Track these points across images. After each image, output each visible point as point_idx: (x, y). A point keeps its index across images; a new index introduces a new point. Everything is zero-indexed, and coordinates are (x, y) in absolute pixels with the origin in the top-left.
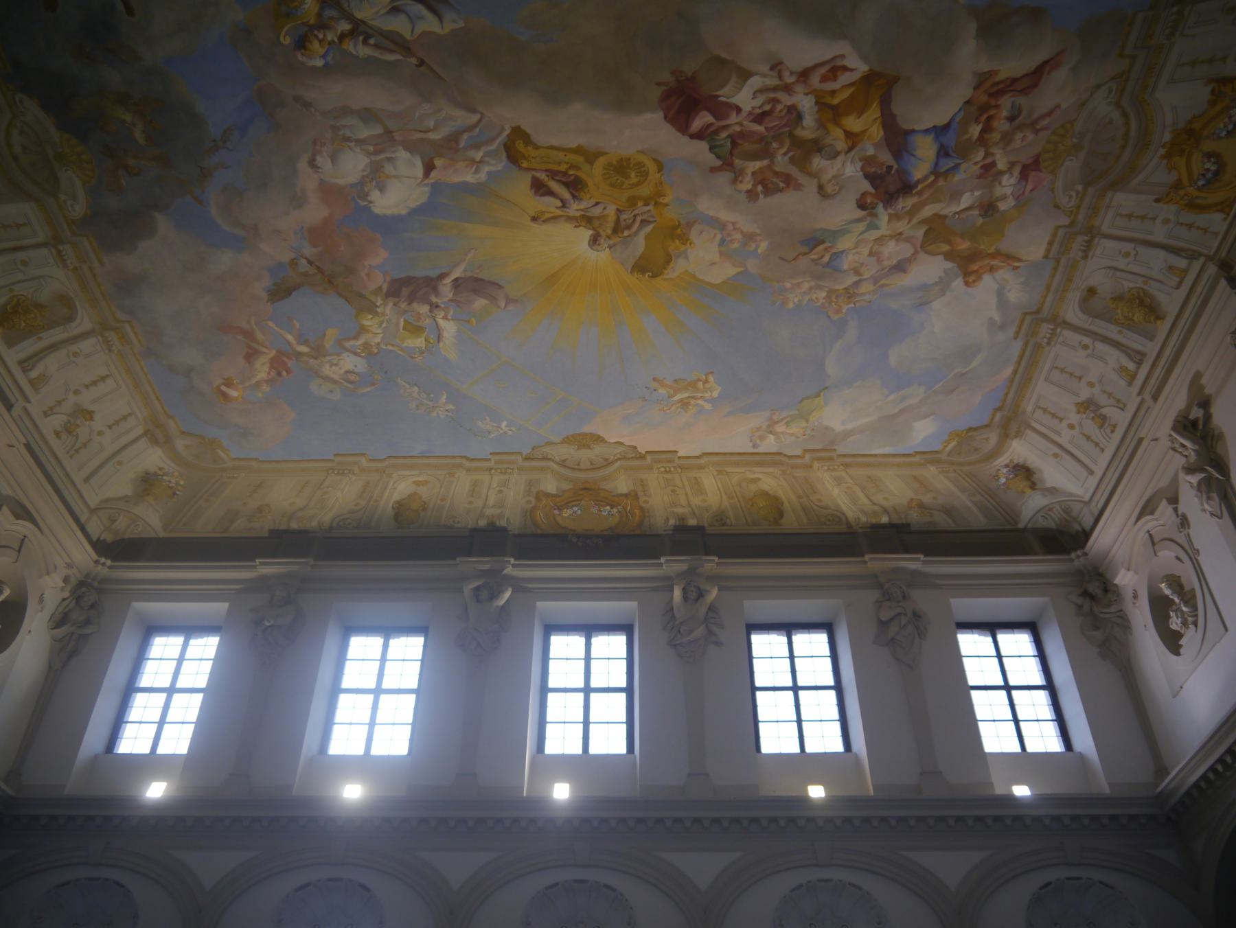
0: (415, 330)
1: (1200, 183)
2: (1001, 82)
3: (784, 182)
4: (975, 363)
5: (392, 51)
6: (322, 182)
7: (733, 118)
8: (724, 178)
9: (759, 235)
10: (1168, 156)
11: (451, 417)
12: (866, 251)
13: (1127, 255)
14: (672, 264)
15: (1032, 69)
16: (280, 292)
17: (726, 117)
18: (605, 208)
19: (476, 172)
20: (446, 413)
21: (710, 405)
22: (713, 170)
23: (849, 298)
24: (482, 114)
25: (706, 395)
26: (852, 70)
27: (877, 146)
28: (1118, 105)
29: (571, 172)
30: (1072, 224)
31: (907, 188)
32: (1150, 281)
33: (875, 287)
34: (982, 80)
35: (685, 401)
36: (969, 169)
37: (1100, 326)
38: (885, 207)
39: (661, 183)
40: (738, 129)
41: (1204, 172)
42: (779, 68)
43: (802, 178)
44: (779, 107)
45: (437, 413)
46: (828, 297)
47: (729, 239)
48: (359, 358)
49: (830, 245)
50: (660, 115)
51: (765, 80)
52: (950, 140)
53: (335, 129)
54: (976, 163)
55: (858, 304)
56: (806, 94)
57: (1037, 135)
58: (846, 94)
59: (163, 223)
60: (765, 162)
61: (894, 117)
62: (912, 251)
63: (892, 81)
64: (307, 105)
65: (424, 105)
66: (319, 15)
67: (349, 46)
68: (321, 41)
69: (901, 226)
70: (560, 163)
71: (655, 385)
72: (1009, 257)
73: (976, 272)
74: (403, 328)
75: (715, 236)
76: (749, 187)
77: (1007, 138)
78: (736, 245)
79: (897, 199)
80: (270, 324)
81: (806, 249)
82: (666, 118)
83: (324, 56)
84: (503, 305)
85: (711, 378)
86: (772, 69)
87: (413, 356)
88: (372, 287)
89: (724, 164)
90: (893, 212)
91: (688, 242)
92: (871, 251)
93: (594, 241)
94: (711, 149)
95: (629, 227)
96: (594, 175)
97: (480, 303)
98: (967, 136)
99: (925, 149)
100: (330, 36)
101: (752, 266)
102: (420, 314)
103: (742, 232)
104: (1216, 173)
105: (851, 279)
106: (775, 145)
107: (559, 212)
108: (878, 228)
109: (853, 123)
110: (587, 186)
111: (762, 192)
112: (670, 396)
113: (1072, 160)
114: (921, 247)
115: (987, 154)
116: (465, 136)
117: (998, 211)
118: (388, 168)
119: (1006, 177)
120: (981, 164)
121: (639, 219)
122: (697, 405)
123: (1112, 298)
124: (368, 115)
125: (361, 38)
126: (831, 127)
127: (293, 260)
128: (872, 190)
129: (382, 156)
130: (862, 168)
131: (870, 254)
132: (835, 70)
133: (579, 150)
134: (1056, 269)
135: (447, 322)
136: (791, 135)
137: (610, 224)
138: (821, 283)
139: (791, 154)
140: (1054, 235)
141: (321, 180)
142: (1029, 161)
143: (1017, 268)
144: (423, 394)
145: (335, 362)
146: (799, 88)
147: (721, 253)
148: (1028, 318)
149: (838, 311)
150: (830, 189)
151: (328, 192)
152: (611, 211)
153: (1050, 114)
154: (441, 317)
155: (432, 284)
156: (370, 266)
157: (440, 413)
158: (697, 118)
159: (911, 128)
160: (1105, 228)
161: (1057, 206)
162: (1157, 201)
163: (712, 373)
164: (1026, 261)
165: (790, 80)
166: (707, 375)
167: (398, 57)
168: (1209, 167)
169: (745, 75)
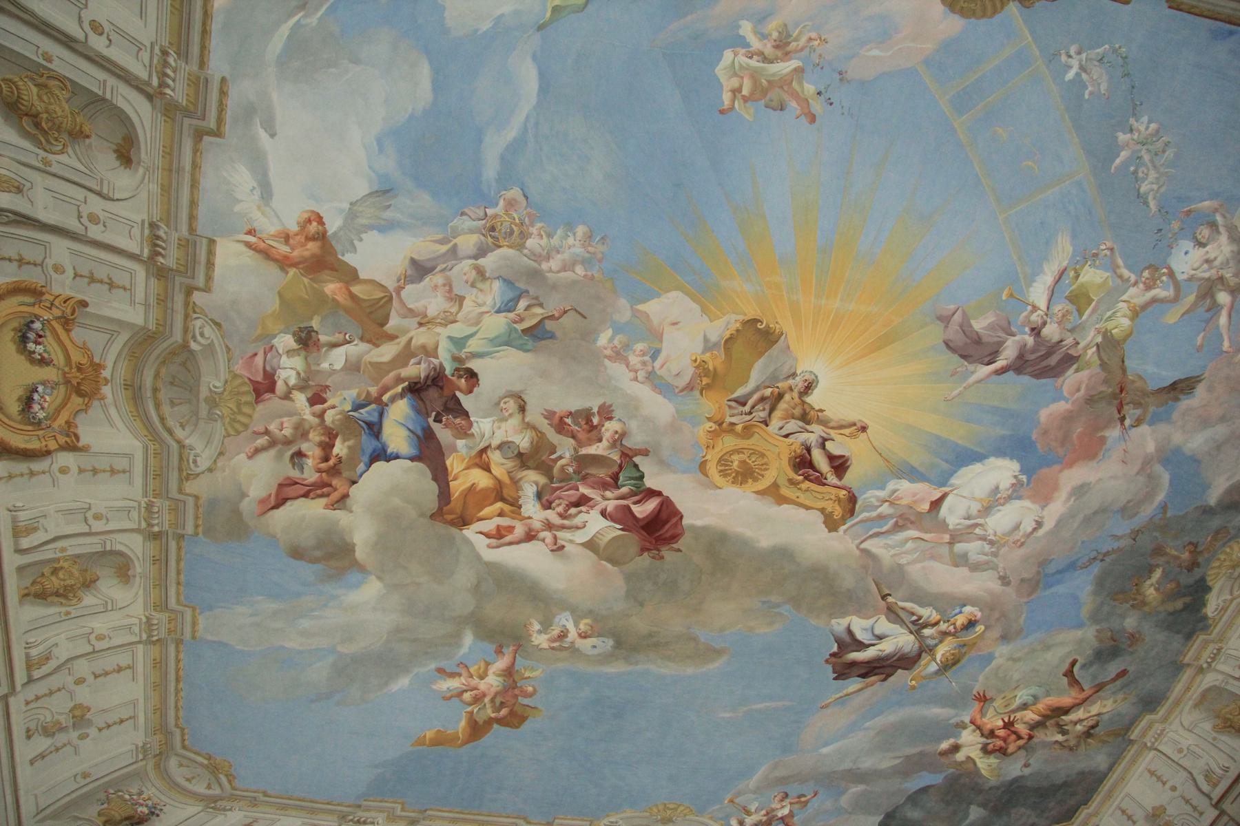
0: (1079, 300)
1: (37, 325)
2: (322, 496)
3: (565, 423)
4: (285, 30)
5: (903, 609)
6: (1043, 508)
7: (611, 505)
8: (635, 440)
9: (609, 358)
10: (98, 367)
11: (1134, 115)
12: (468, 304)
13: (93, 219)
14: (727, 335)
15: (289, 503)
16: (1180, 388)
17: (617, 507)
18: (781, 428)
19: (895, 491)
20: (1135, 125)
21: (741, 32)
22: (645, 453)
23: (493, 229)
24: (858, 547)
25: (742, 59)
26: (481, 533)
27: (454, 449)
28: (182, 446)
29: (801, 478)
30: (189, 291)
31: (415, 389)
32: (40, 165)
33: (455, 241)
34: (342, 501)
35: (779, 53)
36: (340, 402)
37: (91, 77)
38: (441, 365)
39: (708, 447)
40: (608, 494)
41: (40, 340)
42: (555, 547)
43: (544, 425)
44: (560, 509)
45: (1147, 128)
46: (524, 236)
47: (647, 358)
48: (1174, 266)
49: (515, 325)
50: (685, 522)
51: (571, 538)
52: (369, 444)
53: (995, 555)
54: (333, 407)
55: (482, 214)
56: (530, 518)
57: (266, 429)
58: (487, 511)
59: (1213, 498)
60: (584, 451)
61: (435, 479)
62: (403, 293)
63: (438, 515)
64: (1004, 580)
65: (905, 562)
66: (941, 642)
67: (935, 616)
68: (954, 624)
69: (421, 337)
70: (807, 490)
71: (817, 107)
72: (266, 254)
73: (310, 239)
74: (1090, 305)
75: (662, 367)
76: (607, 424)
77: (302, 432)
78: (639, 347)
79: (427, 377)
80: (1226, 345)
81: (549, 325)
82: (682, 517)
83: (961, 612)
84: (959, 313)
85: (726, 98)
86: (563, 547)
87: (1108, 253)
88: (1085, 374)
89: (631, 458)
90: (432, 359)
91: (698, 361)
92: (461, 306)
93: (808, 388)
94: (642, 477)
95: (763, 399)
96: (778, 469)
97: (979, 325)
98: (347, 444)
99: (396, 435)
100: (943, 626)
101: (623, 310)
102: (1059, 323)
103: (627, 367)
104: (24, 339)
105: (488, 262)
106: (571, 470)
107: (832, 432)
108: (450, 338)
109: (481, 479)
110: (790, 459)
111: (593, 414)
112: (799, 71)
113: (215, 387)
114: (391, 299)
115: (321, 416)
116: (884, 529)
117: (294, 335)
118: (975, 507)
119: (292, 381)
120: (326, 405)
121: (747, 408)
122: (763, 37)
123: (88, 137)
124: (961, 560)
125: (921, 622)
126: (506, 479)
127: (1134, 427)
128: (458, 394)
129: (972, 522)
130: (471, 425)
131: (461, 300)
132: (499, 535)
133: (782, 500)
134: (192, 218)
135: (1037, 303)
136: (551, 479)
137: (782, 405)
138: (535, 265)
139: (553, 457)
140: (209, 278)
141: (1042, 509)
142: (267, 396)
143: (249, 233)
144: (1140, 175)
145: (1206, 266)
146: (537, 525)
147: (660, 338)
148: (212, 124)
149: (511, 204)
150: (512, 405)
151: (1044, 498)
152: (775, 423)
153: (257, 451)
154: (1039, 312)
155: (1020, 365)
156: (1067, 402)
157: (1142, 128)
158: (648, 512)
159: (415, 463)
160: (140, 272)
161: (218, 325)
162: (84, 304)
163: (722, 112)
164: (238, 241)
165: (547, 535)
166: (732, 108)
167: (901, 604)
168: (38, 347)
169: (590, 545)
